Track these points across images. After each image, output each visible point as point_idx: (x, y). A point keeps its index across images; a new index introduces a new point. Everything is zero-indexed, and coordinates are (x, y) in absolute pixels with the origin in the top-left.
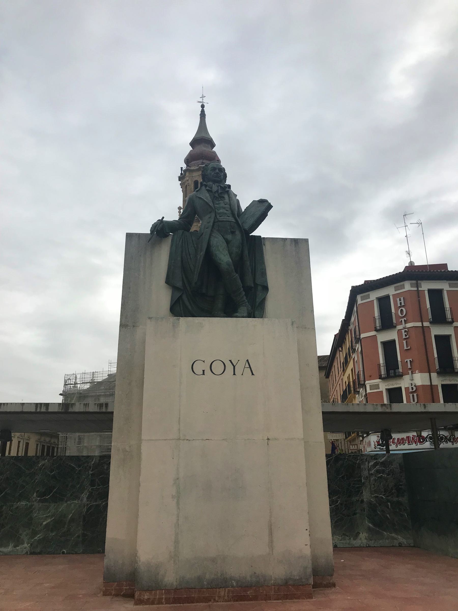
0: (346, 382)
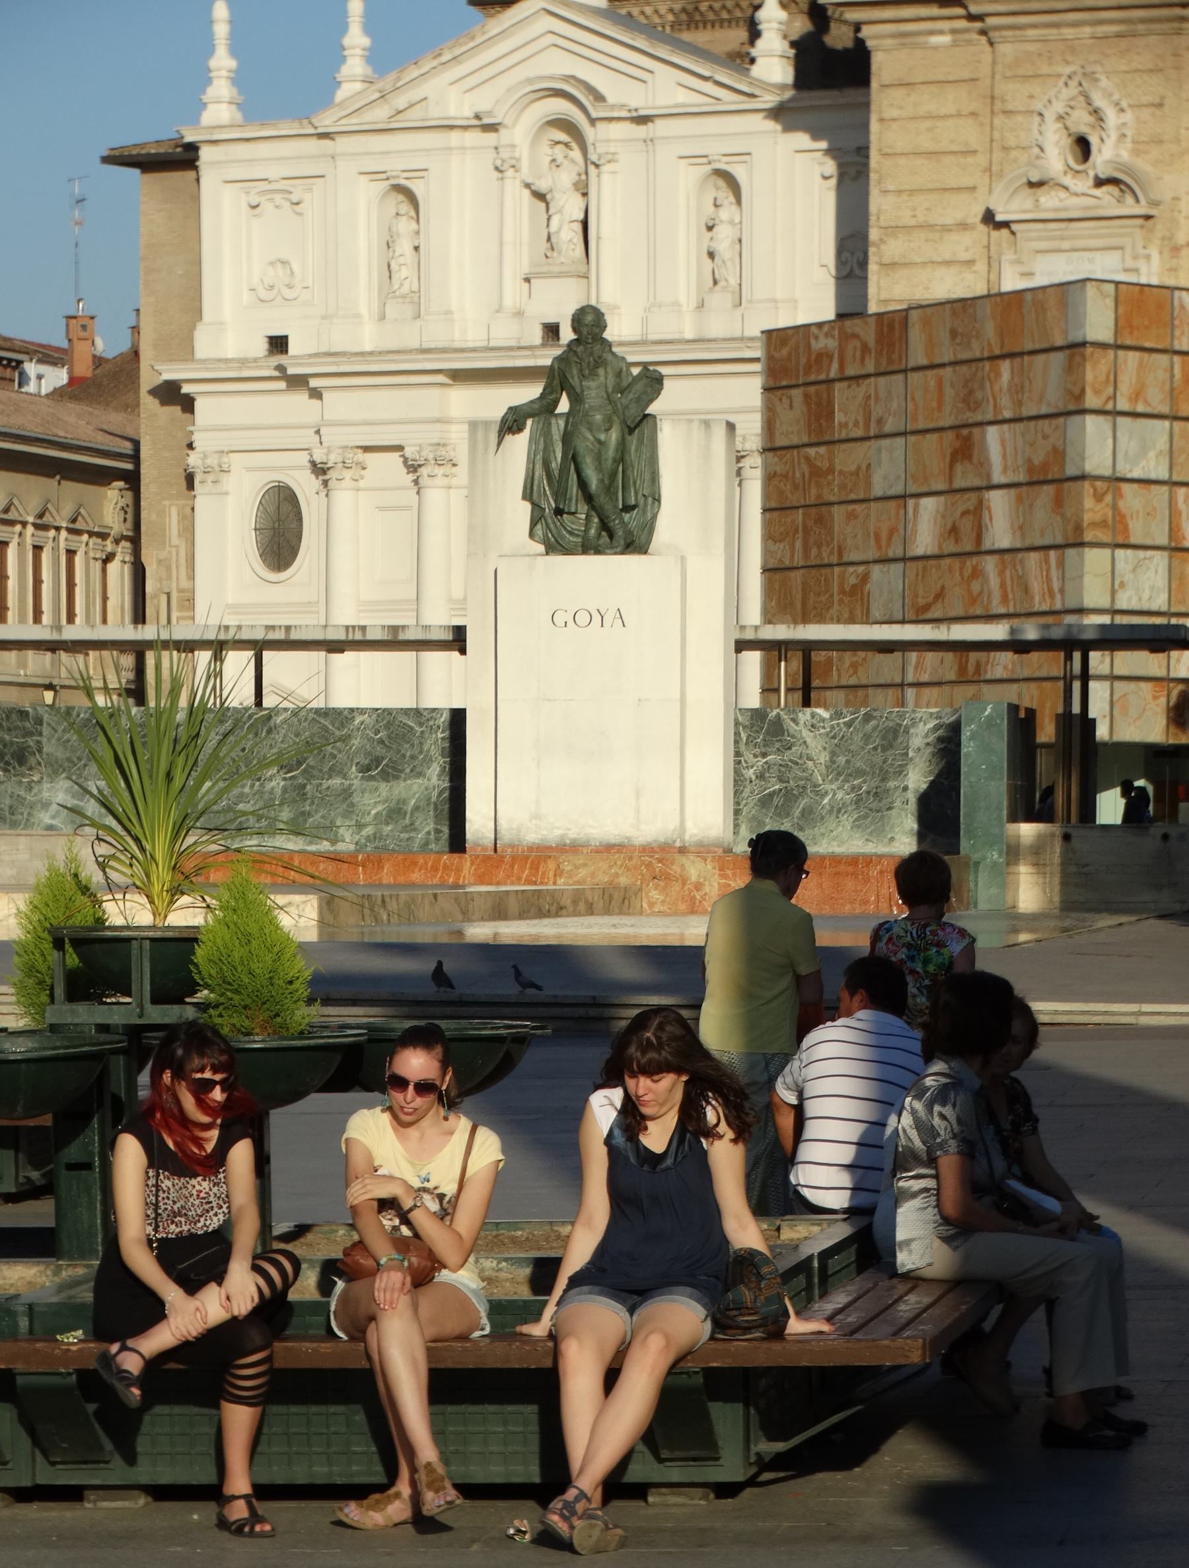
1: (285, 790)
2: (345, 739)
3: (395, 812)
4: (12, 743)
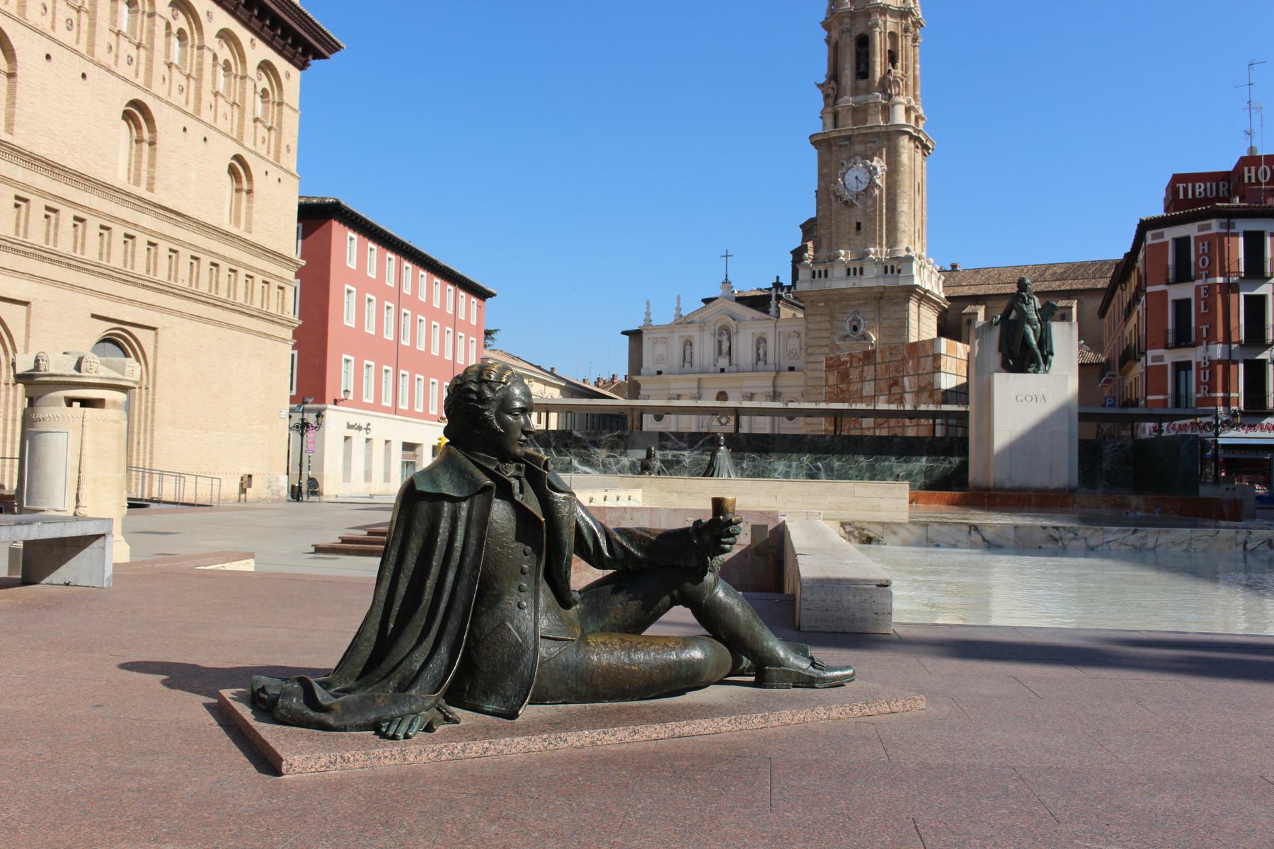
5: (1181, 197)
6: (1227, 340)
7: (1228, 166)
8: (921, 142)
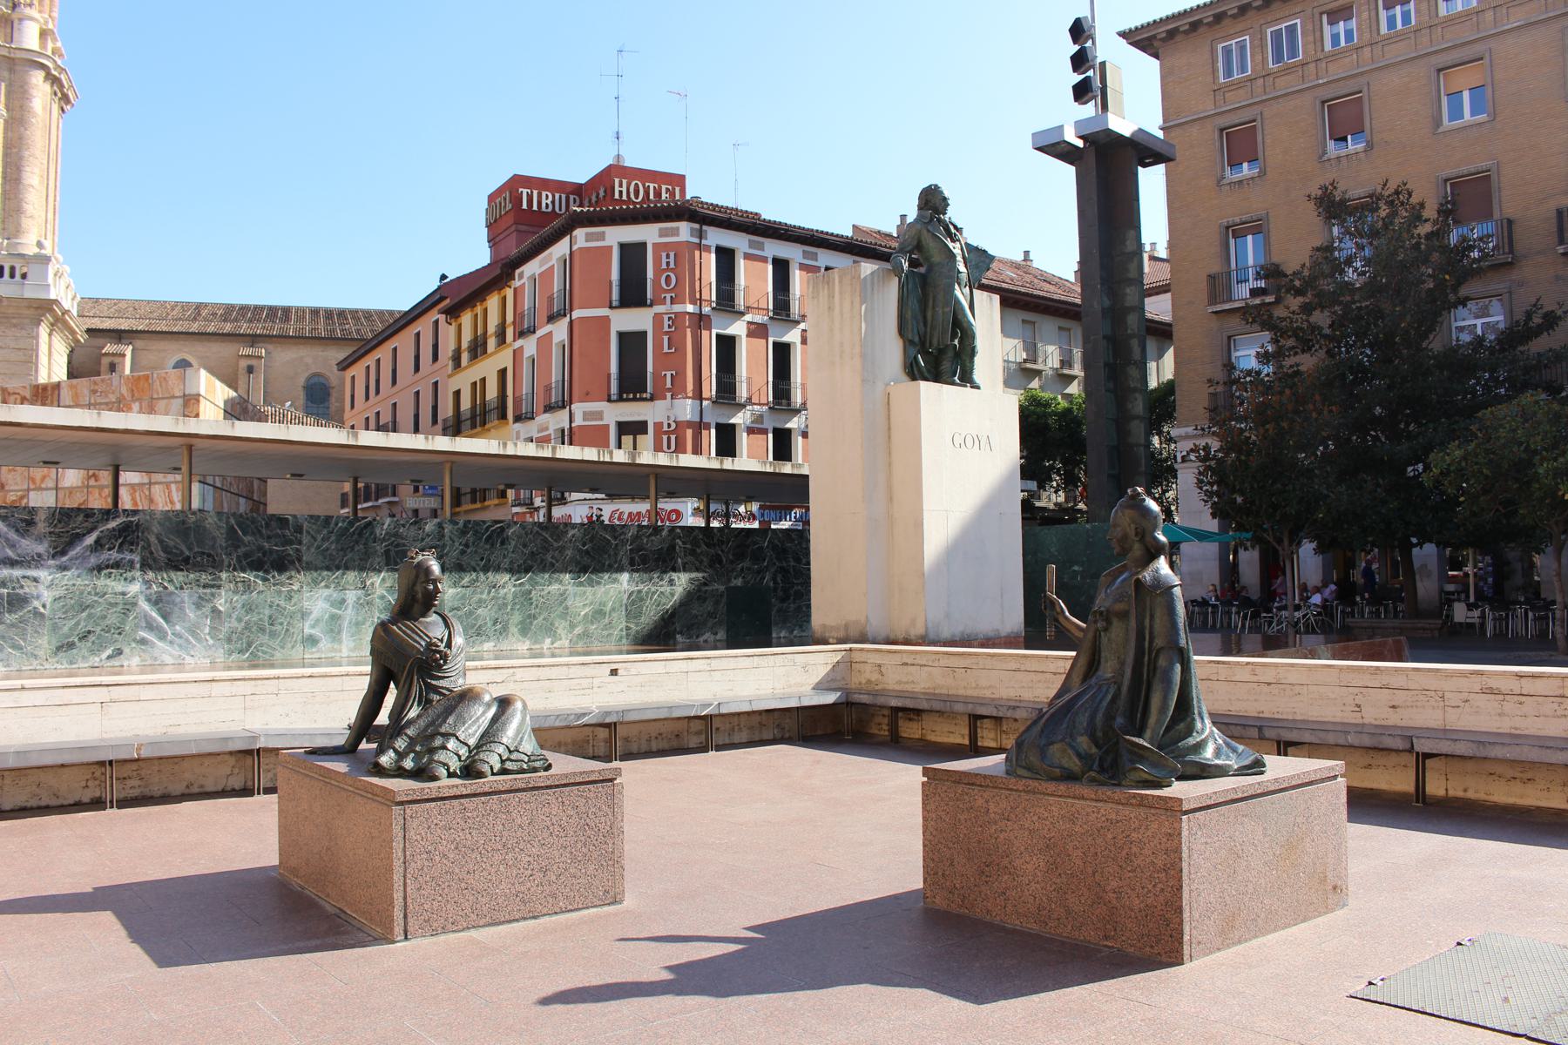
0: (457, 394)
1: (515, 596)
2: (562, 549)
3: (599, 613)
4: (271, 551)
5: (525, 206)
6: (698, 395)
7: (581, 175)
8: (61, 86)
